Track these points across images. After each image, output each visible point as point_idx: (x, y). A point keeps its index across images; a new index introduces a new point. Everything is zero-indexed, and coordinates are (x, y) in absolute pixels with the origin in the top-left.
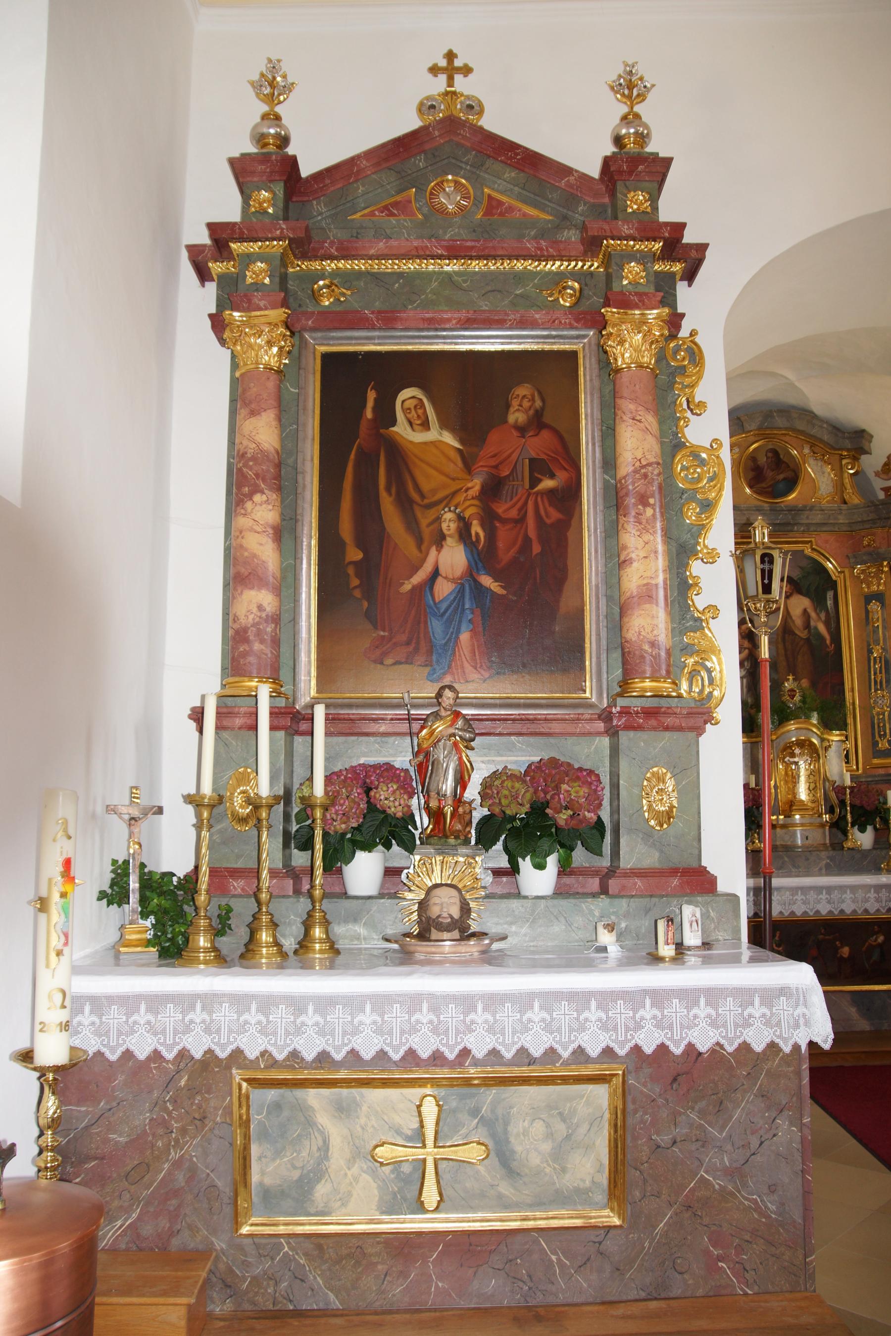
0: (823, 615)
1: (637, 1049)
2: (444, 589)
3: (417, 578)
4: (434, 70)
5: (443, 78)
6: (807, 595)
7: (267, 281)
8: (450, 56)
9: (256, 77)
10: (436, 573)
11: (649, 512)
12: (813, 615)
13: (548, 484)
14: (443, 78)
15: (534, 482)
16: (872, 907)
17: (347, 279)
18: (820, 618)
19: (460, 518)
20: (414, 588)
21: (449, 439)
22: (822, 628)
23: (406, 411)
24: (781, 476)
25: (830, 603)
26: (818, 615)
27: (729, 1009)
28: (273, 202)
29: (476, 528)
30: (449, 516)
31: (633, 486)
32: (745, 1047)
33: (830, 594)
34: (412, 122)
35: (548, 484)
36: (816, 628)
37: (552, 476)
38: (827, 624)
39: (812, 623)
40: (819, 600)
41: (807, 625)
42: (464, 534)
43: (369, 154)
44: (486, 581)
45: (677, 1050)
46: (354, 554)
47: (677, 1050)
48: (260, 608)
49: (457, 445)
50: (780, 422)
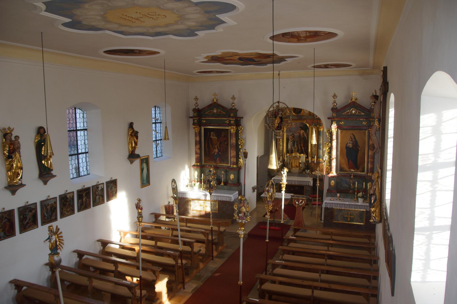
0: (306, 134)
1: (219, 200)
2: (216, 154)
3: (213, 152)
4: (213, 95)
5: (214, 96)
6: (304, 130)
7: (197, 122)
8: (215, 93)
9: (194, 98)
10: (215, 152)
11: (233, 148)
12: (304, 133)
13: (226, 143)
14: (214, 96)
15: (224, 143)
16: (297, 184)
17: (206, 120)
18: (305, 134)
19: (217, 146)
20: (213, 153)
21: (216, 138)
22: (306, 136)
23: (212, 135)
24: (299, 110)
25: (307, 132)
26: (305, 133)
27: (226, 198)
28: (196, 114)
29: (219, 148)
30: (216, 146)
31: (232, 145)
32: (227, 201)
33: (308, 130)
34: (210, 102)
35: (226, 143)
36: (305, 136)
37: (226, 142)
38: (307, 135)
39: (304, 135)
40: (306, 131)
41: (303, 135)
42: (218, 148)
43: (206, 107)
44: (220, 153)
45: (222, 200)
46: (207, 150)
47: (222, 200)
48: (197, 156)
49: (217, 138)
50: (174, 192)
